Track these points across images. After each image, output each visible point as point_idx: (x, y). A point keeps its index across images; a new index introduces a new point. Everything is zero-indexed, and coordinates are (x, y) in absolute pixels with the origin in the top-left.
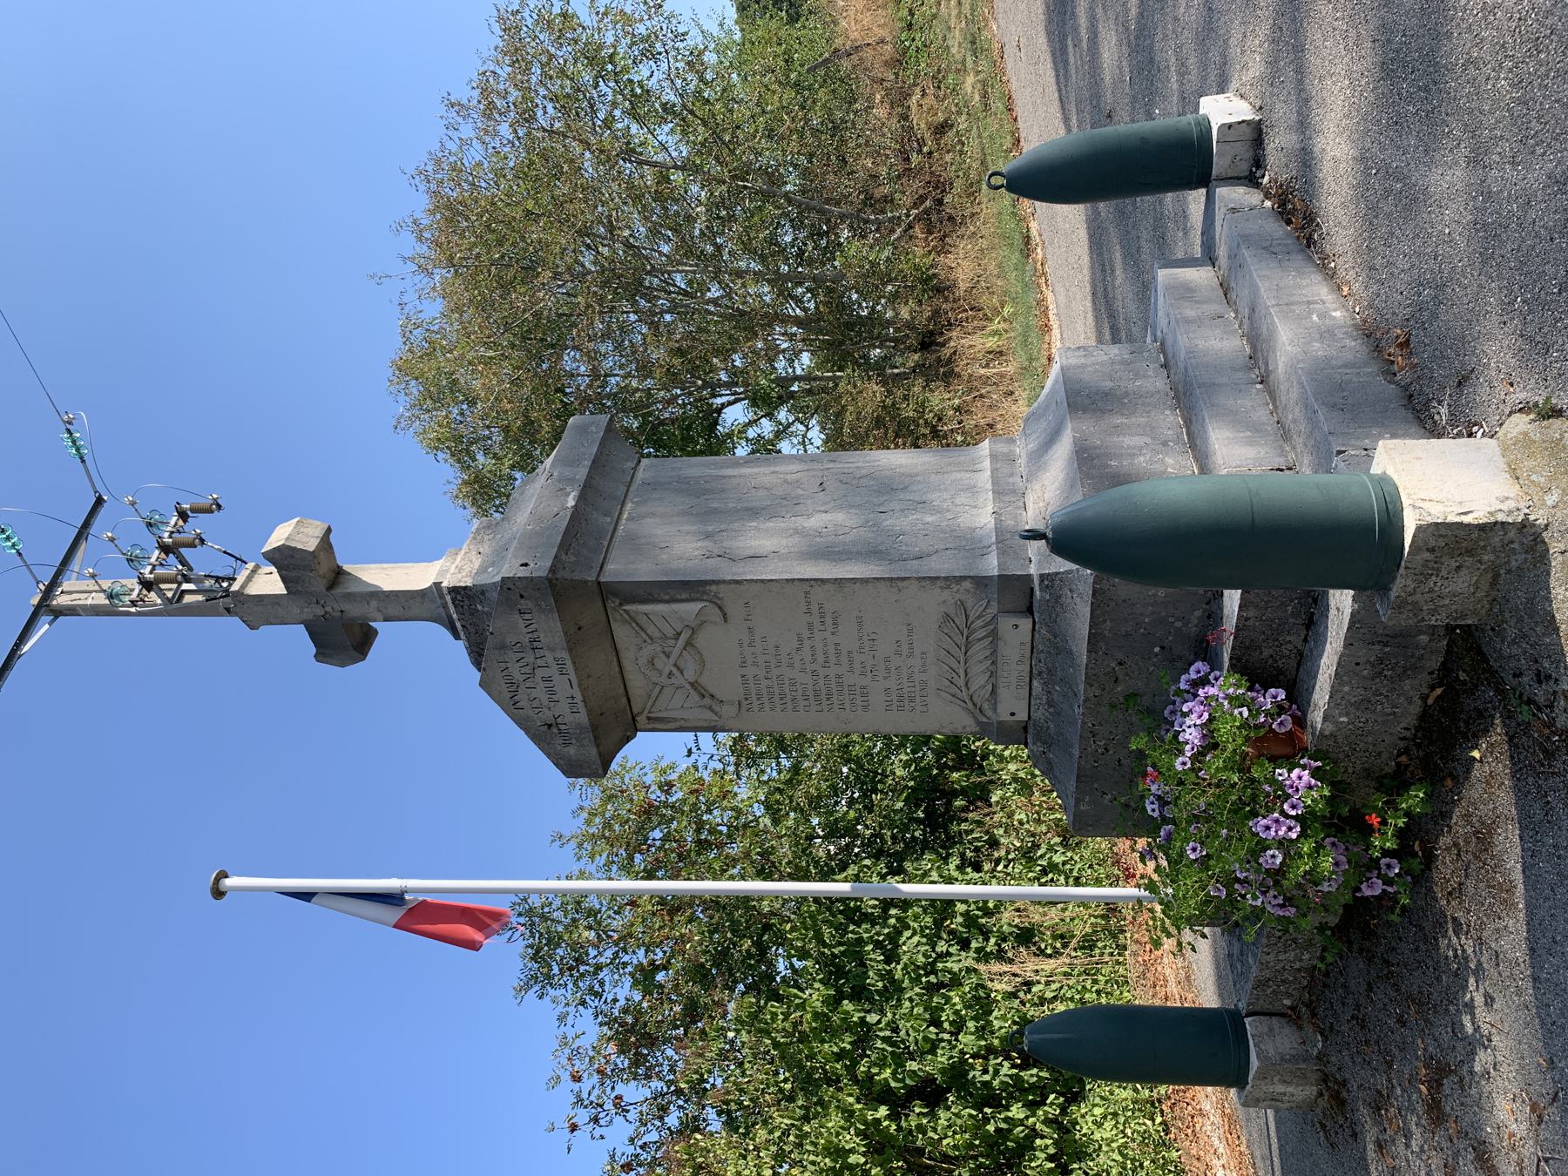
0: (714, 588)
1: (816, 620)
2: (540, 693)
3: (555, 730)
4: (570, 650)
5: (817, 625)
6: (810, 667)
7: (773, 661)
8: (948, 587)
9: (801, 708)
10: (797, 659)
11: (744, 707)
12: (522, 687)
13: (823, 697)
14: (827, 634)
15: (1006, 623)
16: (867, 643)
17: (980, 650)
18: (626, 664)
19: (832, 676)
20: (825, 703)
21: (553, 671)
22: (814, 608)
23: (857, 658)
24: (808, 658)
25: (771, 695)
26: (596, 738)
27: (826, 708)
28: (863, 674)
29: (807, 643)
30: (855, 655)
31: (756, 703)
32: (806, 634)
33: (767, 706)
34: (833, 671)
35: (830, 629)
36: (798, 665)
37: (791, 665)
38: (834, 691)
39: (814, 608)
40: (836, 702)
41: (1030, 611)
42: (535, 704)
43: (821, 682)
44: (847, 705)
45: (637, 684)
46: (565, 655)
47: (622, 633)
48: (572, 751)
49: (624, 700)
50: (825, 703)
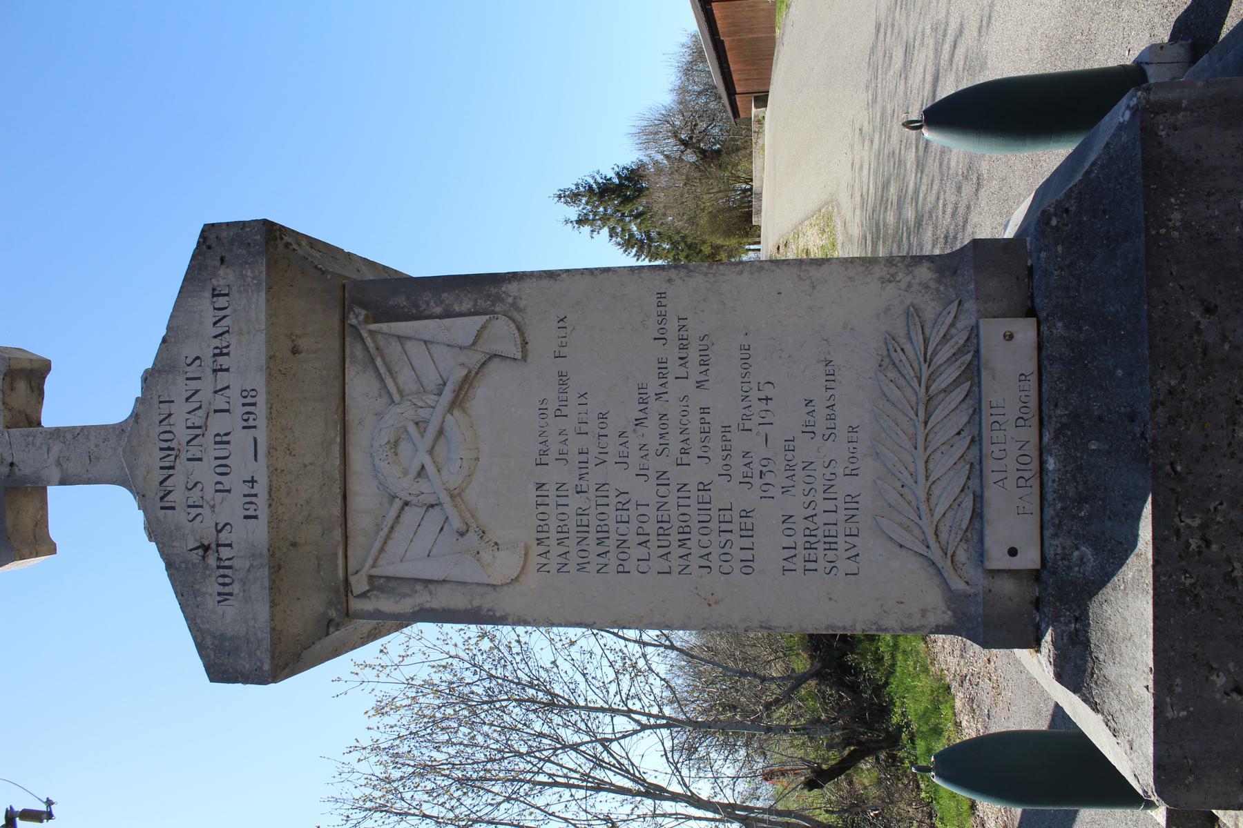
0: (513, 288)
1: (673, 354)
2: (205, 473)
3: (212, 560)
4: (270, 377)
5: (675, 368)
6: (655, 464)
7: (594, 451)
8: (892, 279)
9: (631, 565)
10: (634, 442)
11: (535, 560)
12: (183, 456)
13: (674, 537)
14: (691, 383)
15: (993, 330)
16: (758, 406)
17: (950, 415)
19: (692, 487)
20: (676, 552)
22: (672, 325)
23: (740, 442)
24: (654, 443)
25: (583, 527)
26: (274, 588)
27: (676, 564)
28: (746, 481)
29: (655, 407)
30: (735, 435)
31: (556, 550)
32: (654, 387)
33: (574, 559)
34: (694, 474)
35: (695, 375)
36: (635, 458)
37: (623, 461)
38: (695, 526)
39: (672, 325)
40: (697, 551)
41: (1031, 313)
42: (195, 496)
43: (672, 500)
44: (715, 561)
45: (364, 496)
46: (258, 381)
47: (360, 385)
49: (337, 534)
50: (676, 552)
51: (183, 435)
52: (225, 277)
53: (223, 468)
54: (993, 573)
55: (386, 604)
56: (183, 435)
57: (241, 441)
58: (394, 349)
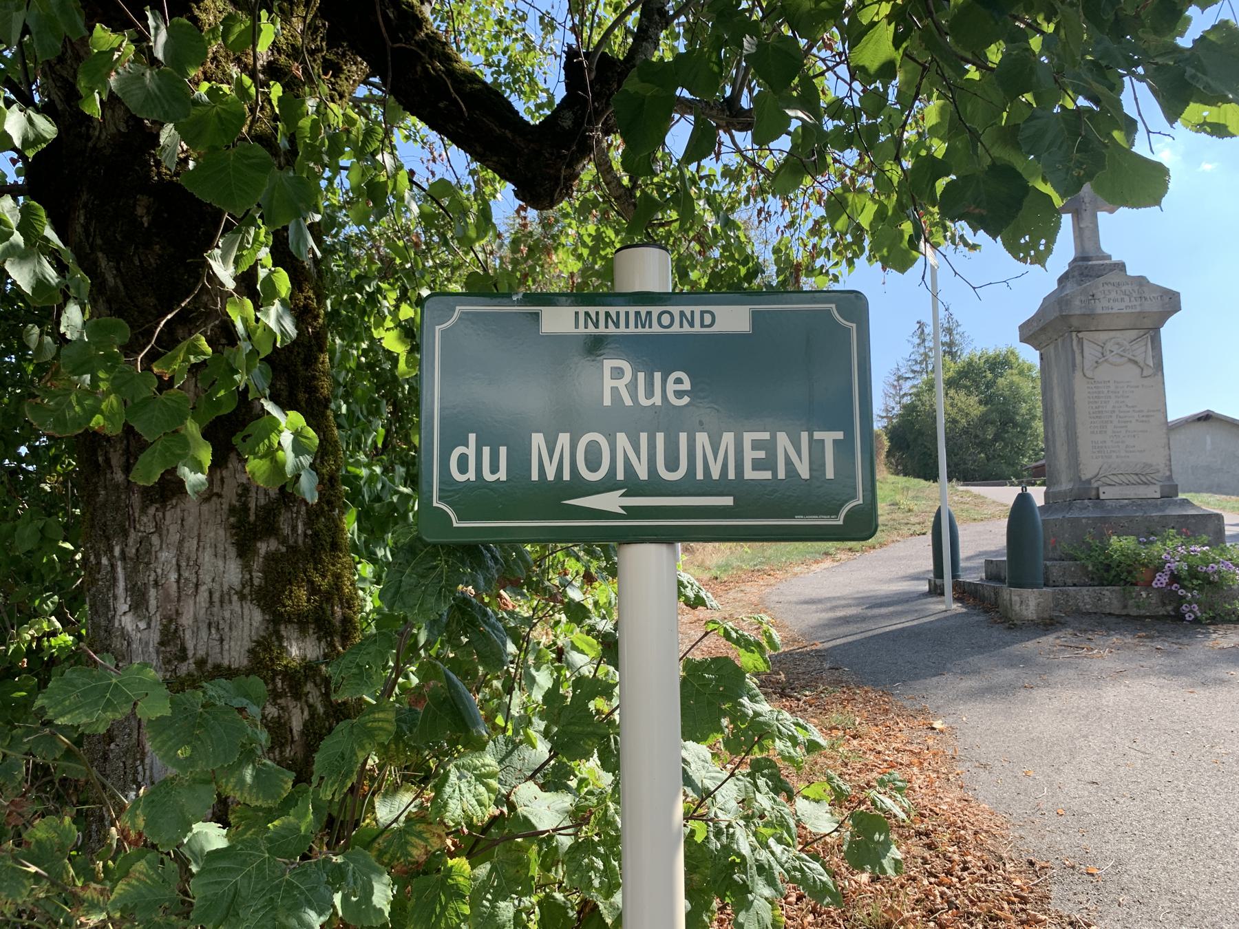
2: (1113, 295)
15: (1158, 490)
17: (1133, 478)
18: (1112, 334)
21: (1127, 303)
45: (1103, 336)
46: (1138, 309)
47: (1133, 334)
48: (1077, 303)
51: (1123, 288)
52: (1167, 300)
53: (1115, 300)
54: (1098, 489)
55: (1075, 342)
56: (1123, 288)
57: (1123, 305)
58: (1143, 343)
